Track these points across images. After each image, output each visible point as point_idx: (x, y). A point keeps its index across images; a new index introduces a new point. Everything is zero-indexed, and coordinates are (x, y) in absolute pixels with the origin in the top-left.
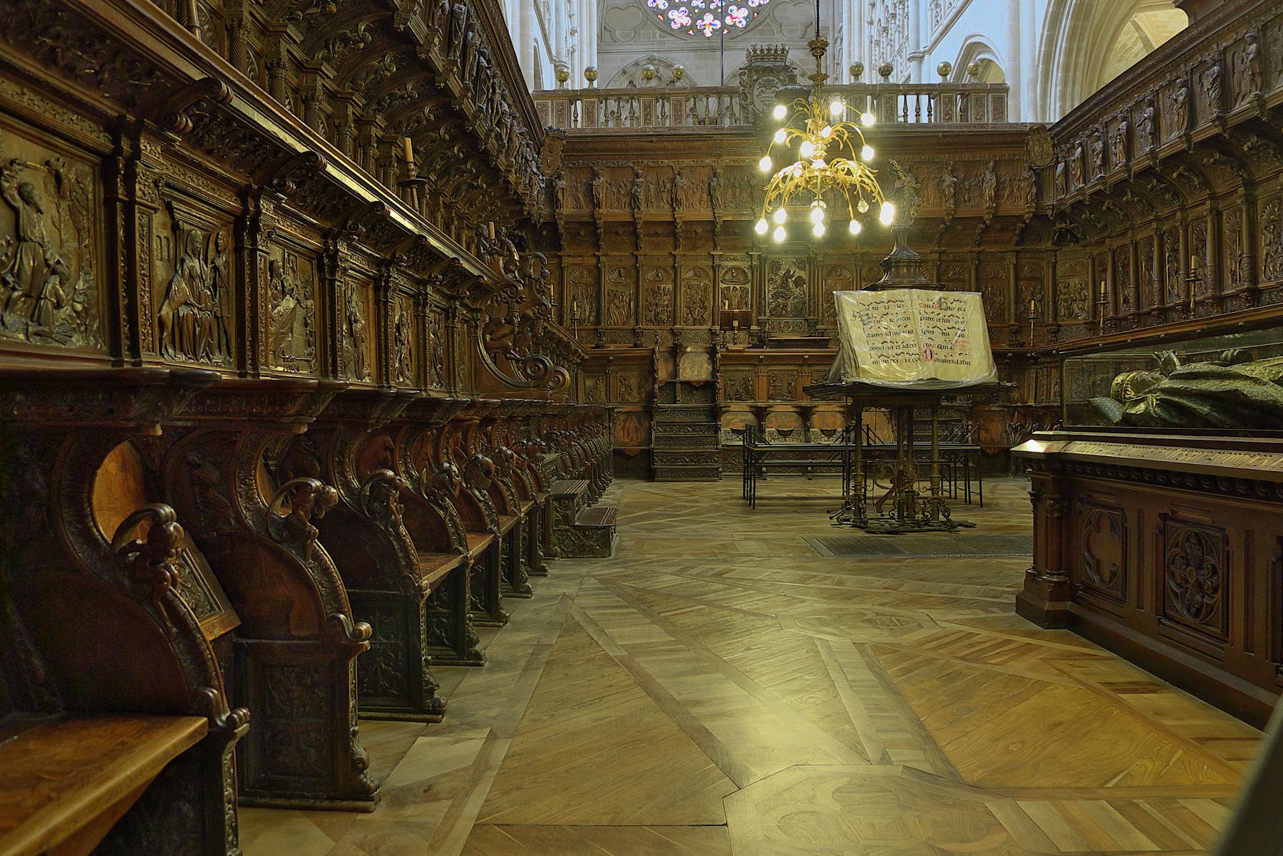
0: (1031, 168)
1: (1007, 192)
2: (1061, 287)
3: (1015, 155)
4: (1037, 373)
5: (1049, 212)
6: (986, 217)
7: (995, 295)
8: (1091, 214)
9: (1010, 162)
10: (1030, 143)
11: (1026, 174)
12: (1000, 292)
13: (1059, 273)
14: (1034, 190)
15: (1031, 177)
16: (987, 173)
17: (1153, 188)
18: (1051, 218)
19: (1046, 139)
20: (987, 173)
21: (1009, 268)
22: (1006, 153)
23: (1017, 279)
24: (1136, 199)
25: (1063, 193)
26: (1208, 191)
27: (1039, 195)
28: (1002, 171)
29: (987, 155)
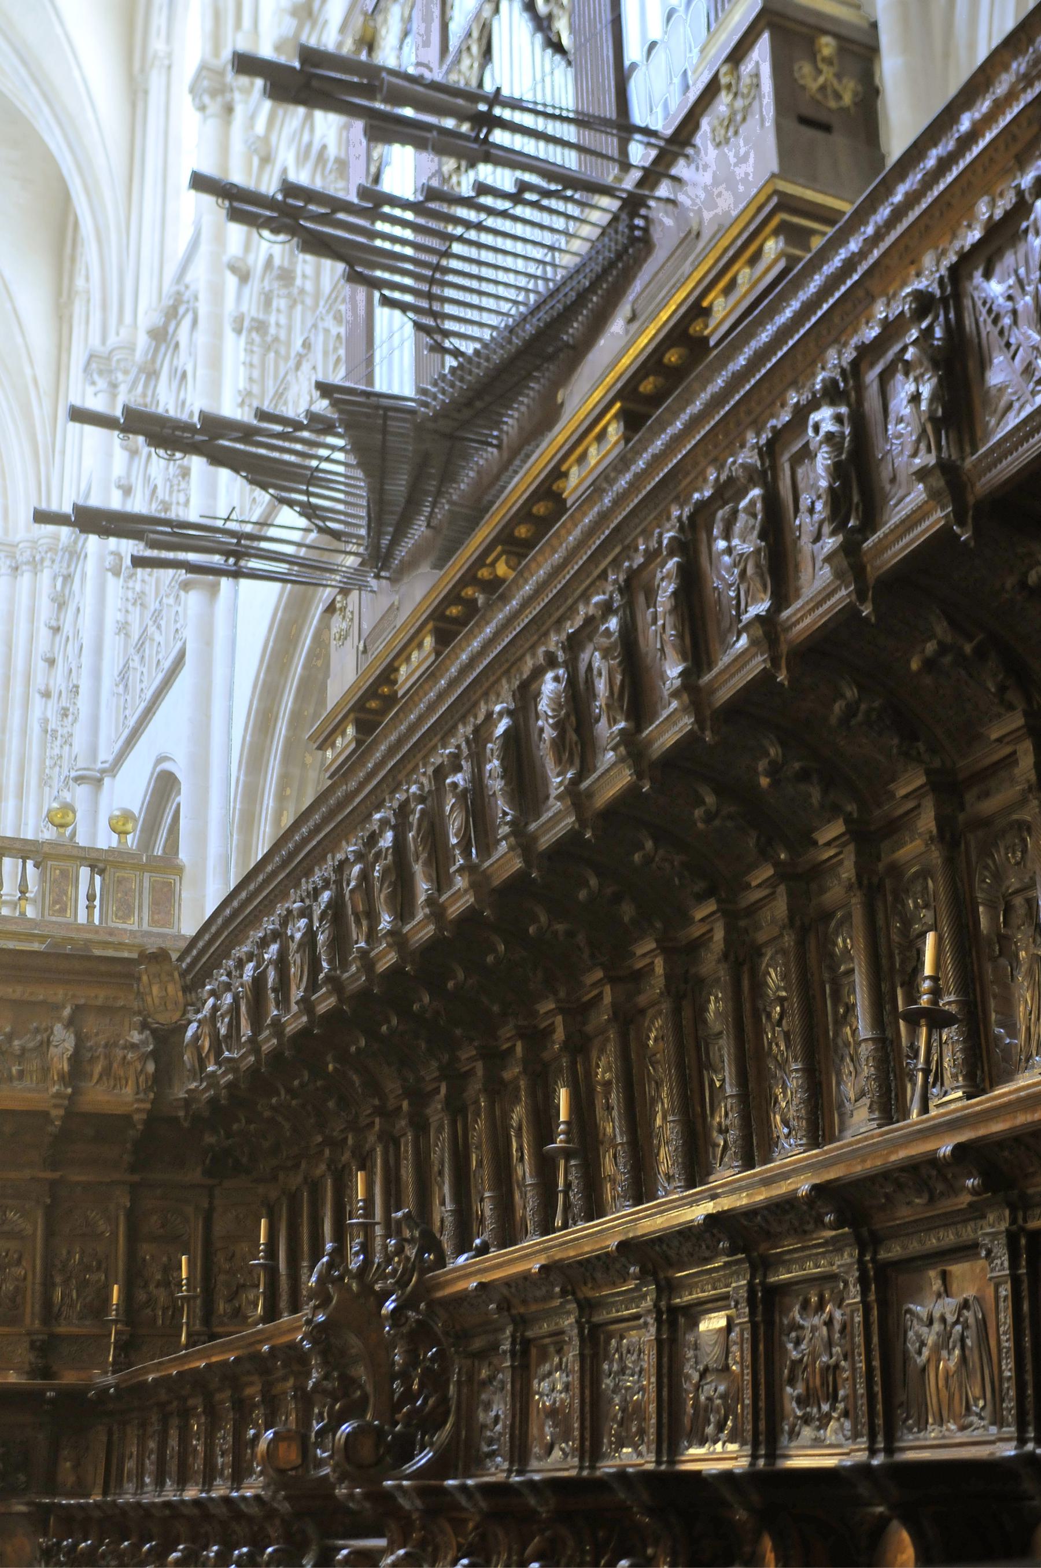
0: (144, 1026)
1: (98, 1069)
2: (220, 1258)
3: (115, 998)
4: (110, 1434)
5: (181, 1114)
6: (55, 1113)
7: (88, 1268)
8: (249, 1122)
9: (105, 1010)
10: (145, 978)
11: (136, 1037)
12: (99, 1264)
13: (219, 1228)
14: (151, 1067)
15: (145, 1043)
16: (58, 1028)
17: (302, 1085)
18: (186, 1125)
19: (171, 975)
20: (58, 1028)
21: (117, 1218)
22: (100, 995)
23: (133, 1238)
24: (294, 1102)
25: (194, 1080)
26: (377, 1102)
27: (161, 1080)
28: (91, 1025)
29: (61, 992)
